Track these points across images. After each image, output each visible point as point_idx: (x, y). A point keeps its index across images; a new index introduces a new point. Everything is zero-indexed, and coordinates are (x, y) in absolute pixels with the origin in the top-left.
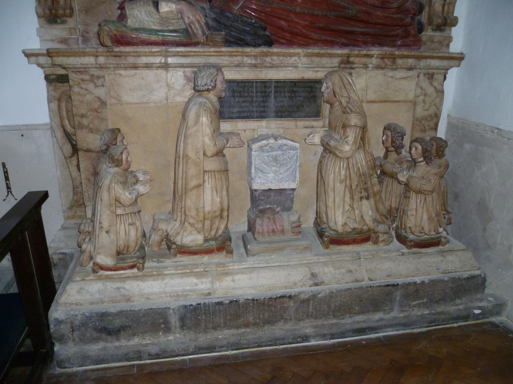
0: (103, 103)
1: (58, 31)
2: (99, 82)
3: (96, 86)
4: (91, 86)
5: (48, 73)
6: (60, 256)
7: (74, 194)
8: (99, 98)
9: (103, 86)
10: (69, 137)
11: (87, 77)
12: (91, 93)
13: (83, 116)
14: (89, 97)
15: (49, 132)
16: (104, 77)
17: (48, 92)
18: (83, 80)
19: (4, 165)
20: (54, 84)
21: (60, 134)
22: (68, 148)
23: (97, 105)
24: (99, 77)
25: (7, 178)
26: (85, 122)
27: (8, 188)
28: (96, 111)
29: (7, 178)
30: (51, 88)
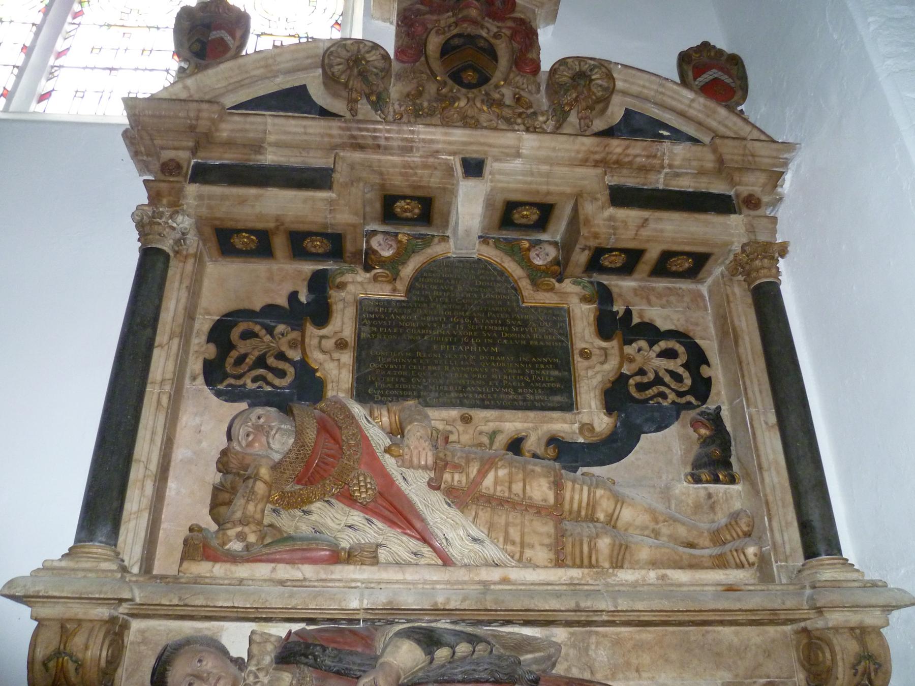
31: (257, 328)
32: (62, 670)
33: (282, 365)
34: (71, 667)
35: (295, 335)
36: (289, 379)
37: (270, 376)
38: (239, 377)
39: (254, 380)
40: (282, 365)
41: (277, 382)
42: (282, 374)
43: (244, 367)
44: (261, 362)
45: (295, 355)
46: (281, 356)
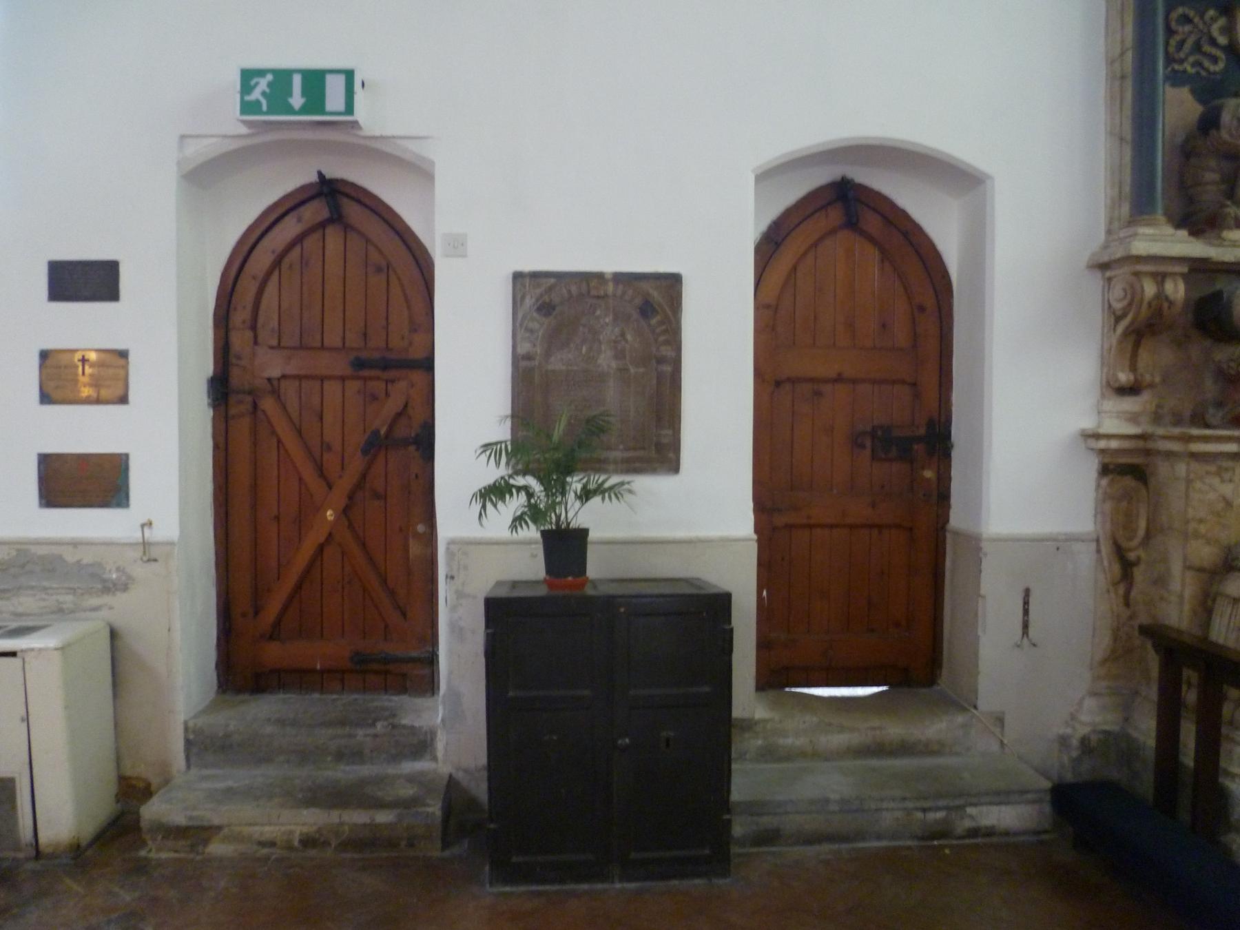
0: (1228, 504)
1: (1129, 404)
2: (1227, 476)
3: (1223, 481)
4: (1216, 481)
5: (1106, 460)
6: (1101, 736)
7: (1115, 640)
8: (1224, 498)
9: (1231, 481)
10: (1120, 552)
11: (1212, 468)
12: (1215, 490)
13: (1201, 521)
14: (1212, 496)
15: (1093, 546)
16: (1234, 470)
17: (1098, 486)
18: (1207, 473)
19: (1027, 592)
20: (1111, 477)
21: (1106, 549)
22: (1117, 568)
23: (1220, 506)
24: (1227, 469)
25: (1026, 612)
26: (1202, 529)
27: (1026, 626)
28: (1218, 515)
29: (1026, 612)
30: (1104, 482)
31: (1191, 14)
32: (1160, 309)
33: (1214, 51)
34: (1166, 305)
35: (1222, 21)
36: (1221, 66)
37: (1207, 64)
38: (1181, 61)
39: (1193, 65)
40: (1214, 51)
41: (1212, 68)
42: (1215, 60)
43: (1182, 55)
44: (1197, 48)
45: (1222, 40)
46: (1213, 42)
